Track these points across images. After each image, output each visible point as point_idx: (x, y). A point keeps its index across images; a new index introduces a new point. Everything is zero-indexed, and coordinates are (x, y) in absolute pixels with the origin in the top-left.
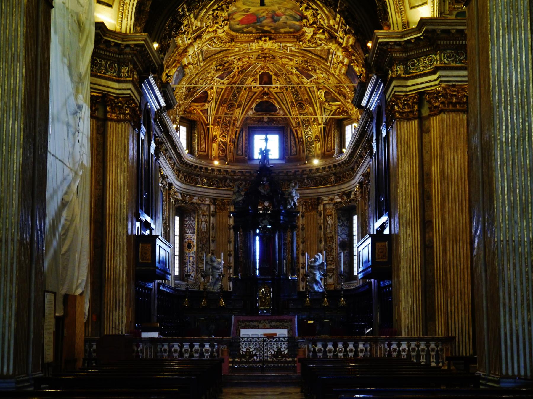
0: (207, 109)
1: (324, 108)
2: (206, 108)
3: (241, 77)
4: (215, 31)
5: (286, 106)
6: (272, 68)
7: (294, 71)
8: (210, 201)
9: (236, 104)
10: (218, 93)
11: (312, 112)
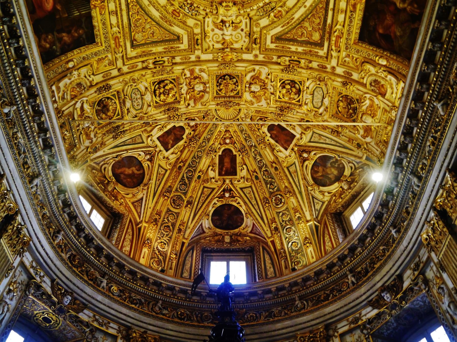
0: (142, 199)
1: (313, 197)
2: (139, 197)
3: (195, 146)
5: (256, 207)
8: (119, 331)
9: (186, 200)
11: (296, 204)
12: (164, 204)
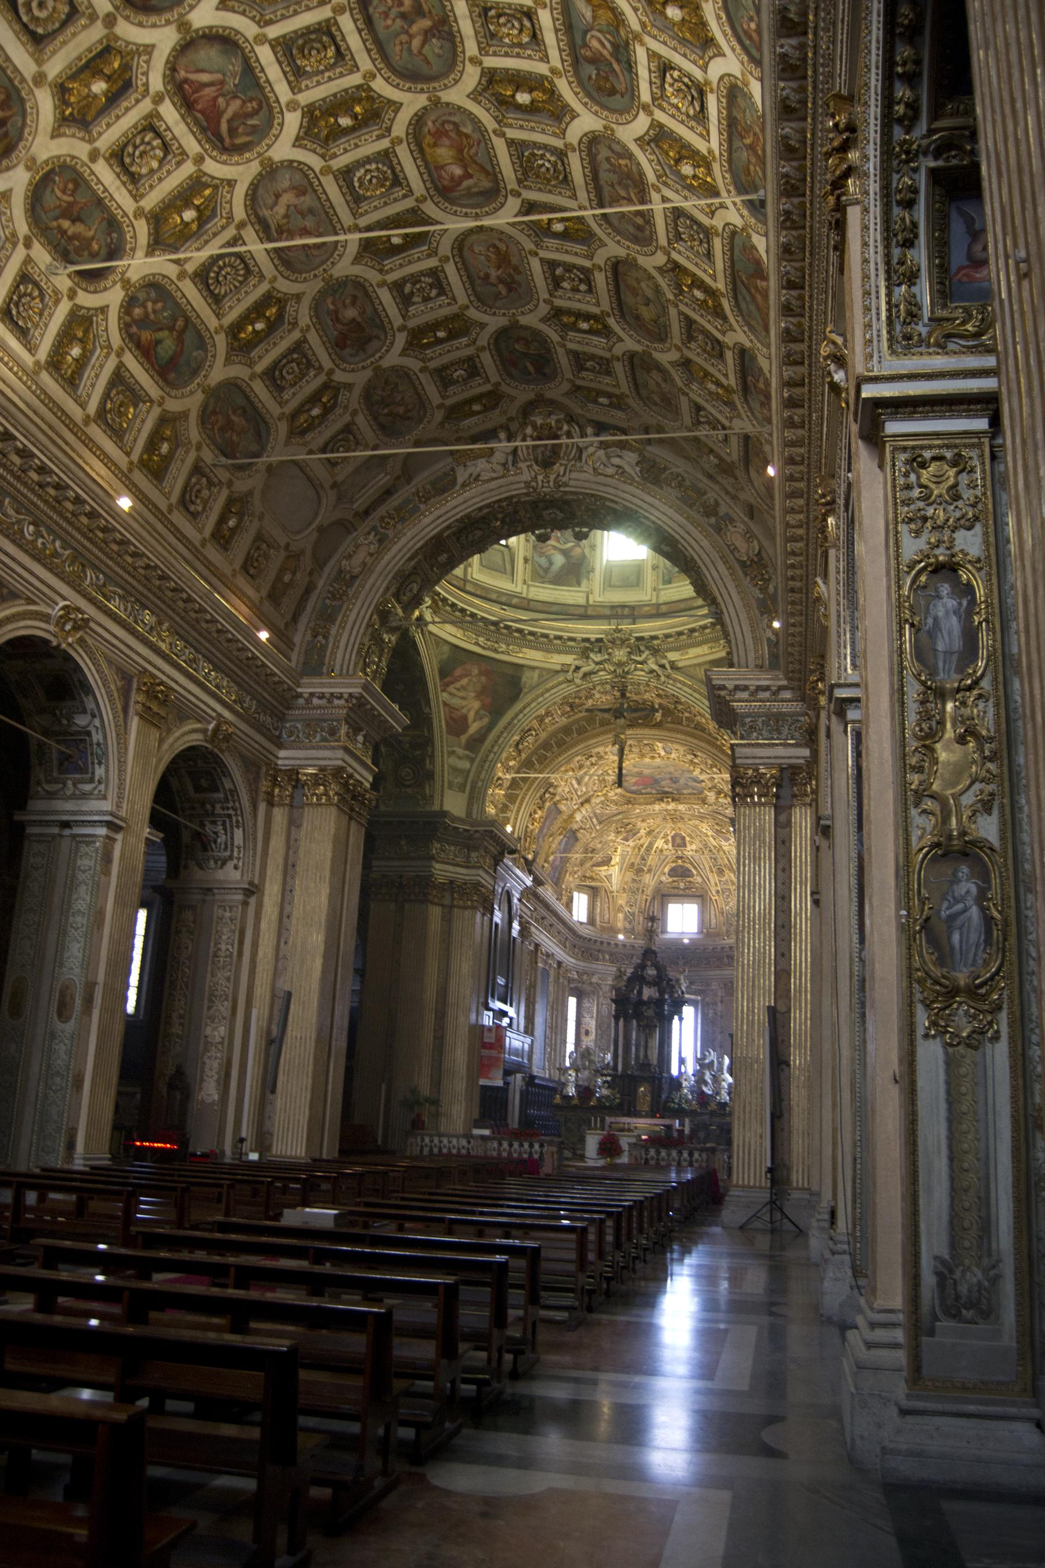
4: (605, 795)
6: (684, 829)
7: (710, 833)
10: (623, 857)
12: (630, 875)
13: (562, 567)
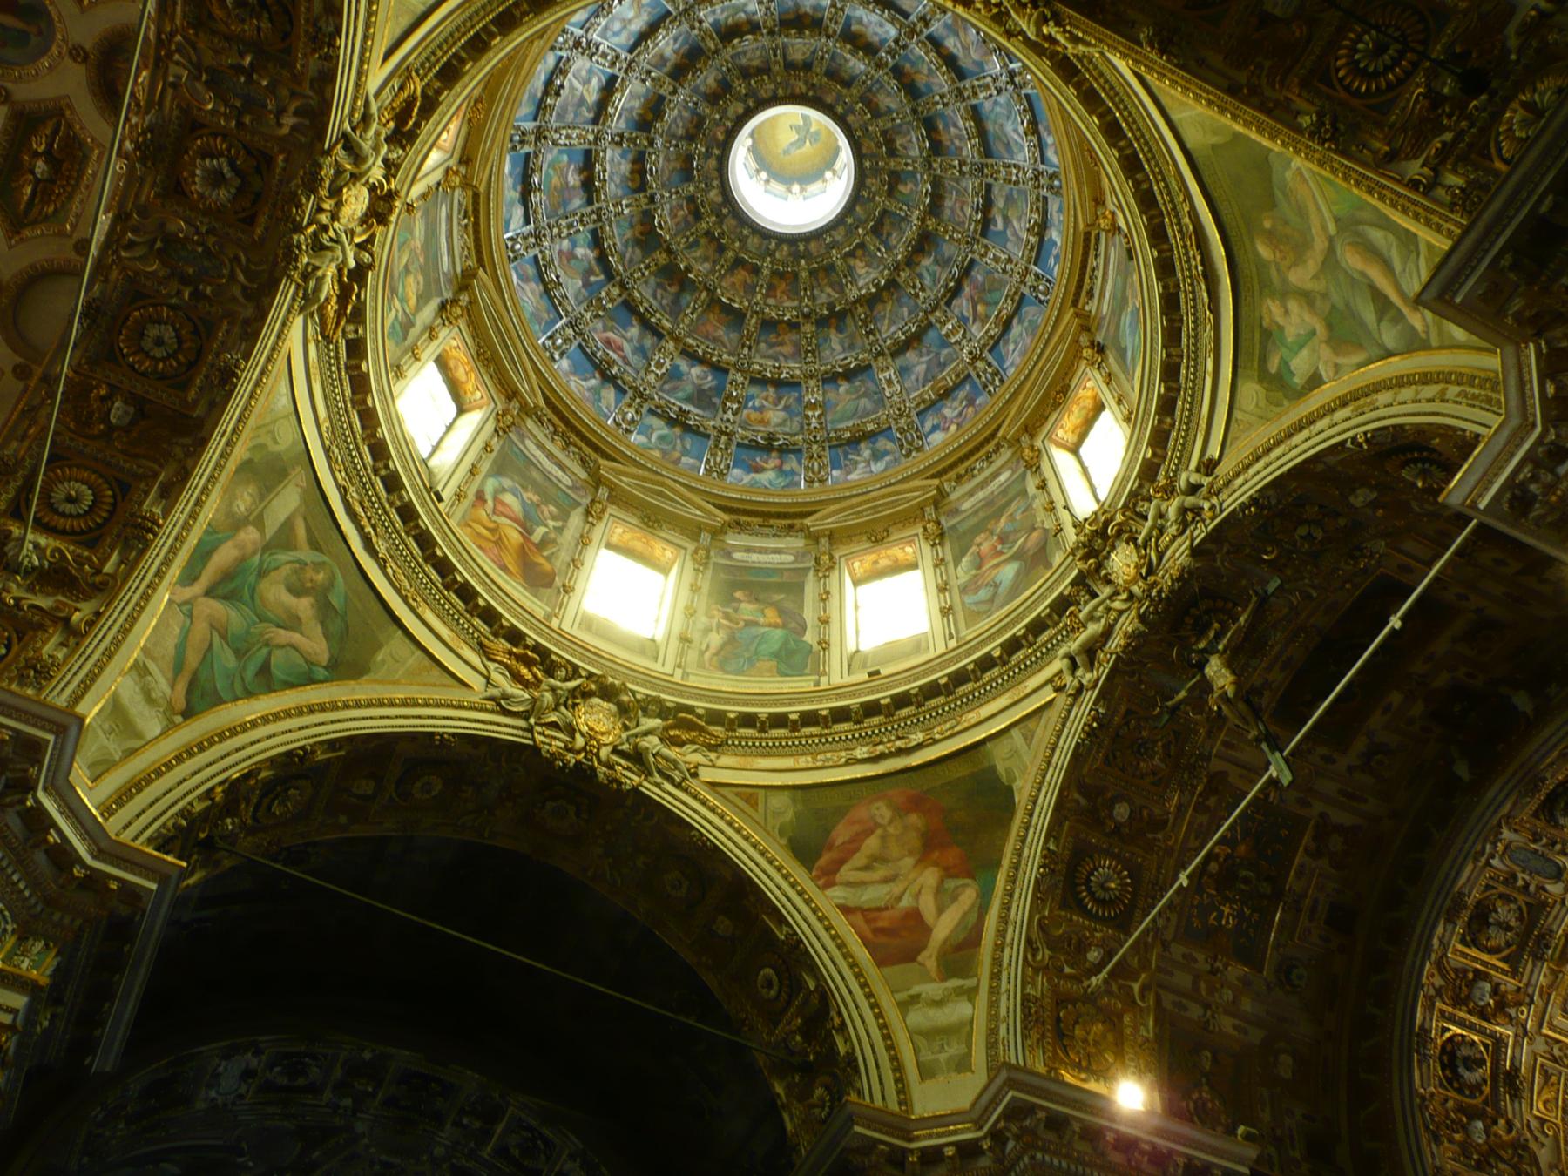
13: (1018, 573)
